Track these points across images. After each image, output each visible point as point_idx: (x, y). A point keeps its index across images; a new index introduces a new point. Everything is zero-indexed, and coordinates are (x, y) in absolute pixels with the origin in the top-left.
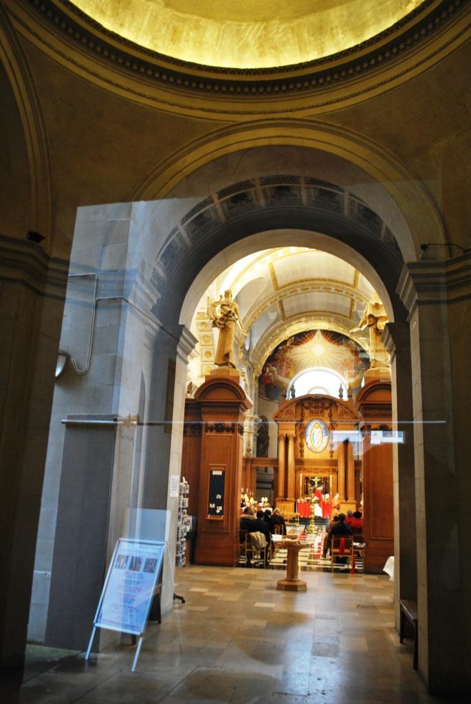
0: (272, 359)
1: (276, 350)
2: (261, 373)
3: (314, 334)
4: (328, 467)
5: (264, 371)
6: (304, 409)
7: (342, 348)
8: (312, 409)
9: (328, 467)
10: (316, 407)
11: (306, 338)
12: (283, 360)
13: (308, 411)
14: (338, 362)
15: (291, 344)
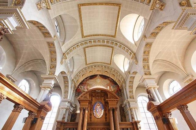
0: (82, 83)
4: (105, 127)
5: (78, 87)
7: (107, 80)
9: (105, 127)
10: (98, 96)
13: (95, 98)
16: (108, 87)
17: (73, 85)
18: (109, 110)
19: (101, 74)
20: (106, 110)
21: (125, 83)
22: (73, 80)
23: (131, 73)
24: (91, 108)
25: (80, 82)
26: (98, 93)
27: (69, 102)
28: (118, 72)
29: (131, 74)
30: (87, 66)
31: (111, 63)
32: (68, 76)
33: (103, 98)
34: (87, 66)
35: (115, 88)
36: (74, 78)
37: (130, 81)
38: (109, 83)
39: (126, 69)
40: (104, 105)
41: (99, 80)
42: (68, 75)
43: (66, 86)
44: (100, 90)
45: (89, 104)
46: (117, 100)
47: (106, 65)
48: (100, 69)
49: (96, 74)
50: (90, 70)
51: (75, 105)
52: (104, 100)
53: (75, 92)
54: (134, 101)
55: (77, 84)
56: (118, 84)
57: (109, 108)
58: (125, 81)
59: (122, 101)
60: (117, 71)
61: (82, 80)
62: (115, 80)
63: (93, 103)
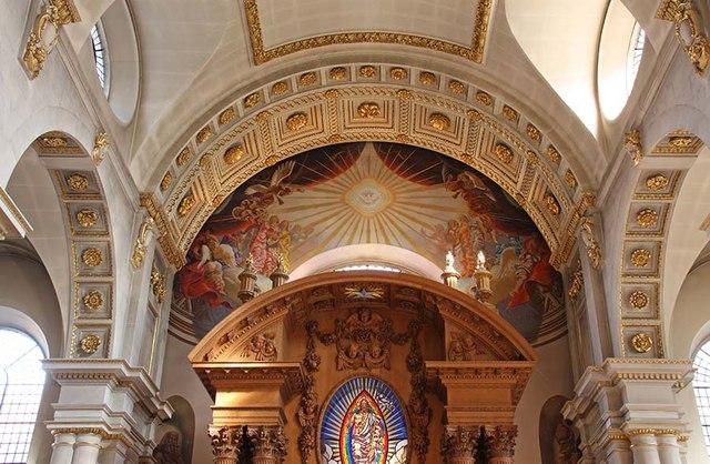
0: (222, 223)
1: (239, 195)
2: (185, 261)
3: (356, 155)
5: (193, 257)
6: (318, 343)
7: (442, 194)
8: (345, 343)
11: (331, 165)
12: (259, 226)
14: (429, 232)
15: (285, 181)
16: (450, 257)
17: (148, 239)
18: (449, 448)
19: (390, 135)
20: (428, 443)
21: (600, 227)
22: (144, 198)
23: (653, 140)
24: (304, 432)
25: (209, 208)
26: (361, 307)
27: (121, 383)
28: (546, 126)
29: (651, 147)
30: (261, 70)
31: (485, 42)
32: (102, 173)
33: (401, 353)
34: (261, 70)
35: (511, 264)
36: (152, 181)
37: (642, 213)
38: (465, 219)
39: (616, 97)
40: (410, 408)
41: (372, 190)
42: (98, 159)
43: (96, 262)
44: (373, 285)
45: (286, 398)
46: (515, 371)
47: (435, 56)
48: (382, 92)
49: (350, 135)
50: (296, 99)
51: (176, 401)
52: (415, 365)
53: (168, 293)
54: (663, 378)
55: (185, 229)
56: (542, 227)
57: (450, 429)
58: (600, 203)
59: (570, 374)
60: (532, 114)
61: (226, 190)
62: (512, 189)
63: (320, 389)
